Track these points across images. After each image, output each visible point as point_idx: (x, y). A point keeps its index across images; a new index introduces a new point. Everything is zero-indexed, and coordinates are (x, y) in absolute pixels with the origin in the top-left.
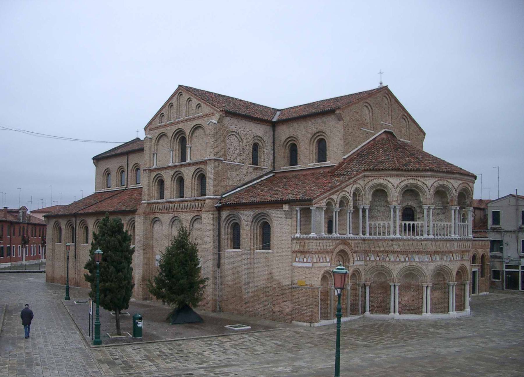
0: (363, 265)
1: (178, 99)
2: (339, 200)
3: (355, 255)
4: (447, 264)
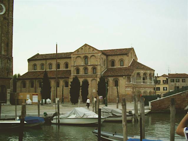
1: (85, 47)
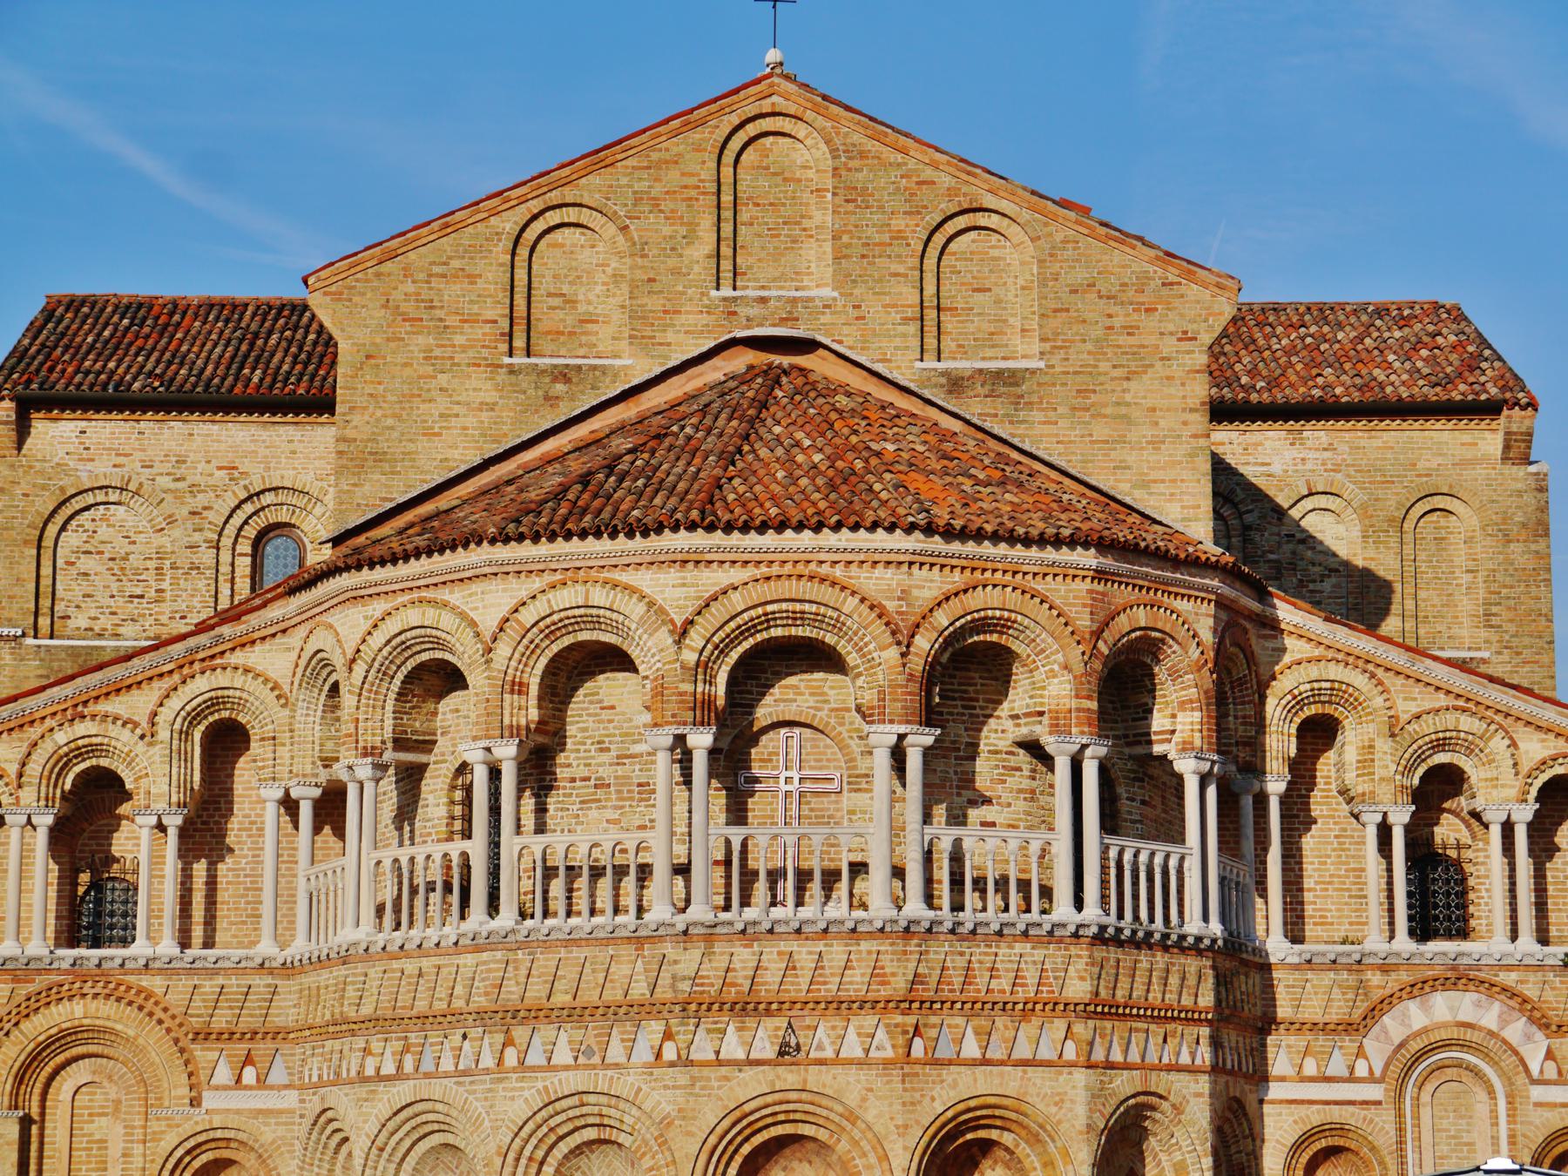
0: (291, 1112)
2: (34, 768)
3: (203, 1054)
4: (625, 1084)
